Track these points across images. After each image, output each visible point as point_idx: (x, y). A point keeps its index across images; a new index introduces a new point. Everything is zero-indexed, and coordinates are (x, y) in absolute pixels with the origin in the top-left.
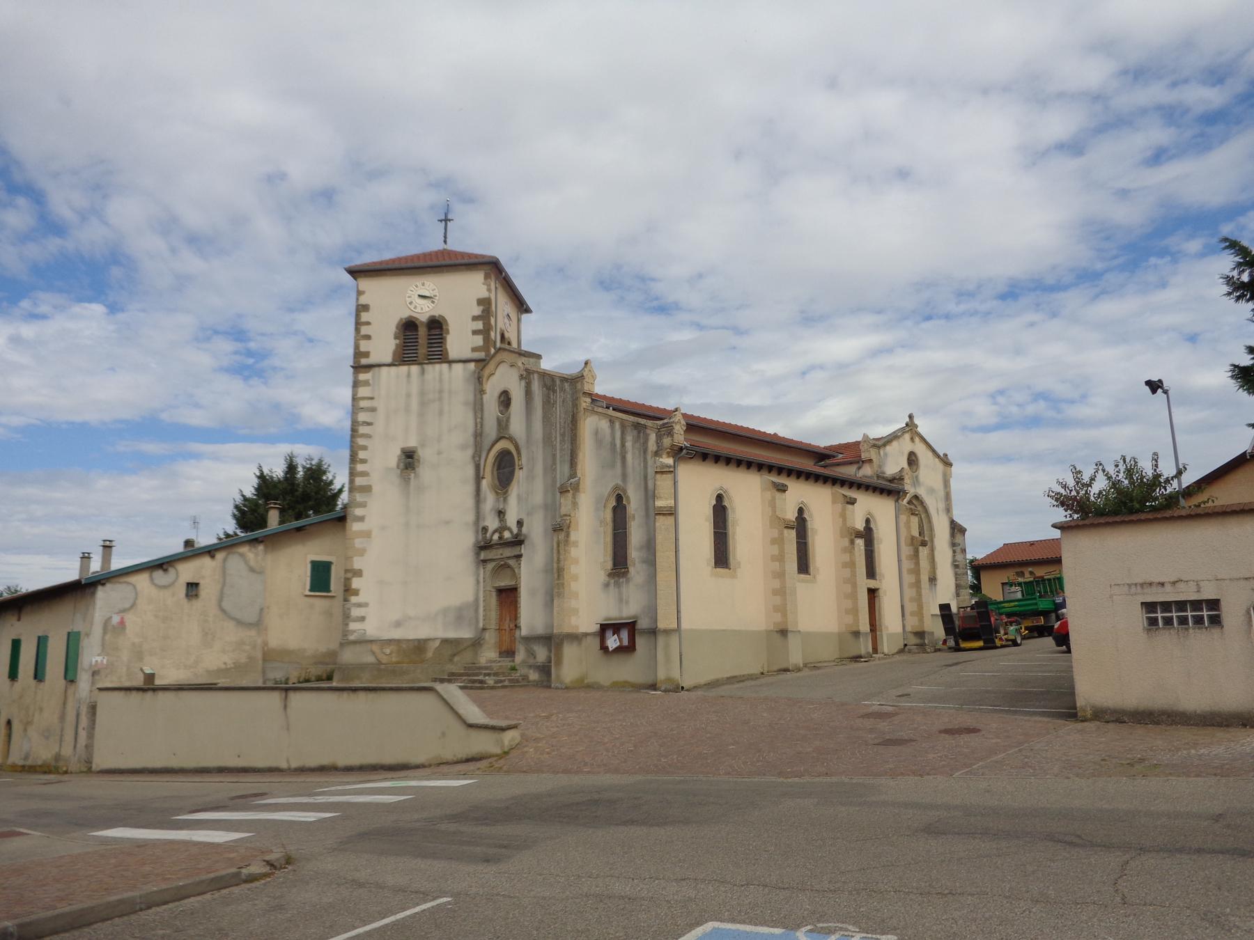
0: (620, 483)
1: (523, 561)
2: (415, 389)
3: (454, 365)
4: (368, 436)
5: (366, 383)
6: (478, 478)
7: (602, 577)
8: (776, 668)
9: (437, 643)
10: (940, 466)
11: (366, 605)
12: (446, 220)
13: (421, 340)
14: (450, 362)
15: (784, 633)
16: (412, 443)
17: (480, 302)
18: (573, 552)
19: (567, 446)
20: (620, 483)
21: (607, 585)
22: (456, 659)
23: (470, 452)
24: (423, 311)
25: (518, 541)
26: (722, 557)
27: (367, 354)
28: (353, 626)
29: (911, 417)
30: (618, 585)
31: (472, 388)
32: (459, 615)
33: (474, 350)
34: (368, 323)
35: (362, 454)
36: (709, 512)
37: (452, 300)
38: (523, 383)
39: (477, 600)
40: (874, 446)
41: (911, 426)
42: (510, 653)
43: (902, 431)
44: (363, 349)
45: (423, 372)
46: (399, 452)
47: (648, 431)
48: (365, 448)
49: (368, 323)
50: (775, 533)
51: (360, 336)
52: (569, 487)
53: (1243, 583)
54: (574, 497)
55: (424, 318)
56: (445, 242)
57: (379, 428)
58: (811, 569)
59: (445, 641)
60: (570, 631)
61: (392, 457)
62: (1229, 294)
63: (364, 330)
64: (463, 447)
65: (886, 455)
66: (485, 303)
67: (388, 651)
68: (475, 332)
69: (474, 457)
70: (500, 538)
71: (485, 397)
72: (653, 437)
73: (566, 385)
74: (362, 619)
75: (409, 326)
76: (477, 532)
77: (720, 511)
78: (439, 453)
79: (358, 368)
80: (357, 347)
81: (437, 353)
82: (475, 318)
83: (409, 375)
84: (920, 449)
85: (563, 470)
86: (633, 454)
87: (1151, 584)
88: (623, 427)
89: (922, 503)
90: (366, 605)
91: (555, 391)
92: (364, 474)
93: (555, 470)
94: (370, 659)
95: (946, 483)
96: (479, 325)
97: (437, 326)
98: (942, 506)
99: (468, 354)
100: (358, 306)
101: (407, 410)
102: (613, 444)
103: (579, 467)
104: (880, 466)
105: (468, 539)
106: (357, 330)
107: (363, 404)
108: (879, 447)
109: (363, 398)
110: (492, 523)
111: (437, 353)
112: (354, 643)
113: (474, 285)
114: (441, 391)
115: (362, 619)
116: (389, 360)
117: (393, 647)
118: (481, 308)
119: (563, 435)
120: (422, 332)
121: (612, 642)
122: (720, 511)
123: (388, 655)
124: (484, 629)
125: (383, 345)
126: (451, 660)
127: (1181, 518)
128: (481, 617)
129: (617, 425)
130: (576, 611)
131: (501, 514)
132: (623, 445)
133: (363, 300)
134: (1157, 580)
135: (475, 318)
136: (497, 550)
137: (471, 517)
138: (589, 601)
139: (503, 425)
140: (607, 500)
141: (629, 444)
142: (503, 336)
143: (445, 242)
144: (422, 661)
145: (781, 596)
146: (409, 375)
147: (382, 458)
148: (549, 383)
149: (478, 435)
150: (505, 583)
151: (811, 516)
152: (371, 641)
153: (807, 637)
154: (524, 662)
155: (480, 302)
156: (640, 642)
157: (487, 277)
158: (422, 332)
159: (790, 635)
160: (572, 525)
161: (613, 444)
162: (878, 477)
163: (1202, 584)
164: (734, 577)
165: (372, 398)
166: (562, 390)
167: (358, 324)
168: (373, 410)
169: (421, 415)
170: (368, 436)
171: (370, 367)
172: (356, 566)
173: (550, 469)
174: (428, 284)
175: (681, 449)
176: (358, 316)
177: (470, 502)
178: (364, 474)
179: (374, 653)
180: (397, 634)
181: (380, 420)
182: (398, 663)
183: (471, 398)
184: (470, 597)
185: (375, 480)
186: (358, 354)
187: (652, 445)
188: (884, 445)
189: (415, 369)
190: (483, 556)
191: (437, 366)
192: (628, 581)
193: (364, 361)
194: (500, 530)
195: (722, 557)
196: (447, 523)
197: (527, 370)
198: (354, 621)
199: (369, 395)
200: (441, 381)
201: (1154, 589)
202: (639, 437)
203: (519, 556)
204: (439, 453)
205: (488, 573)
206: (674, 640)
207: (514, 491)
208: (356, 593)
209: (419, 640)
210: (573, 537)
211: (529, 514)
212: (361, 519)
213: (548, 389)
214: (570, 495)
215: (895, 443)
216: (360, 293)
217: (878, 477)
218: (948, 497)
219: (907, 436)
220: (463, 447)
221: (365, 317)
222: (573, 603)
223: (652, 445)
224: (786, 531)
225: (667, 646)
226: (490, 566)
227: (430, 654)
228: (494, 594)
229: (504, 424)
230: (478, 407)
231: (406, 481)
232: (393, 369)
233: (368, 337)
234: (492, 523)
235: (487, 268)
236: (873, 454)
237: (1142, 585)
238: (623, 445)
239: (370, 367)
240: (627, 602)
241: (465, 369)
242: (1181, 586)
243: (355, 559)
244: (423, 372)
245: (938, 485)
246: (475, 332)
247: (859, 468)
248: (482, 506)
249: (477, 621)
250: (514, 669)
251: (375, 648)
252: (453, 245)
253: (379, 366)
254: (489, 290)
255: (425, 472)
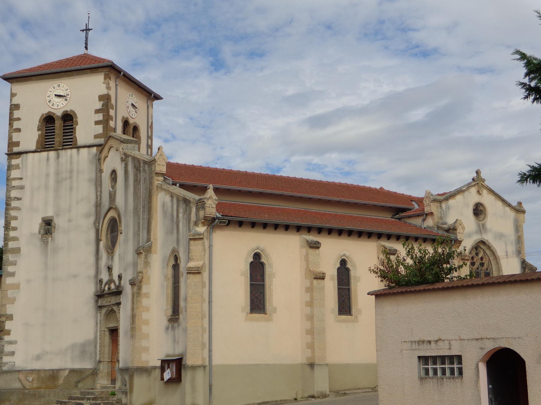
0: (176, 246)
1: (122, 306)
2: (52, 171)
3: (81, 150)
4: (18, 209)
5: (17, 167)
6: (98, 240)
7: (165, 322)
8: (307, 395)
9: (66, 373)
10: (512, 214)
11: (15, 342)
12: (87, 30)
13: (57, 130)
14: (78, 148)
15: (312, 365)
16: (50, 213)
17: (101, 98)
18: (145, 302)
19: (146, 216)
20: (176, 246)
21: (167, 328)
22: (80, 385)
23: (92, 219)
24: (58, 107)
25: (118, 293)
26: (258, 302)
27: (17, 144)
28: (5, 359)
29: (478, 172)
30: (173, 328)
31: (94, 168)
32: (83, 350)
33: (96, 137)
34: (19, 119)
35: (13, 224)
36: (246, 269)
37: (81, 96)
38: (123, 165)
39: (96, 338)
40: (435, 201)
41: (478, 181)
42: (113, 381)
43: (469, 186)
44: (14, 140)
45: (58, 156)
46: (40, 221)
47: (192, 205)
48: (16, 218)
49: (19, 119)
50: (307, 283)
51: (13, 130)
52: (143, 250)
53: (474, 342)
54: (146, 257)
55: (59, 113)
56: (86, 48)
57: (25, 203)
58: (353, 311)
59: (72, 371)
60: (140, 365)
61: (36, 225)
62: (526, 97)
63: (16, 125)
64: (88, 216)
65: (448, 208)
66: (105, 99)
67: (31, 379)
68: (97, 123)
69: (95, 223)
70: (109, 289)
71: (103, 174)
72: (194, 210)
73: (146, 166)
74: (13, 353)
75: (48, 120)
76: (97, 284)
77: (257, 267)
78: (69, 221)
79: (11, 155)
80: (10, 138)
81: (69, 142)
82: (97, 111)
83: (48, 159)
84: (487, 200)
85: (143, 234)
86: (183, 222)
87: (423, 342)
88: (178, 200)
89: (489, 247)
90: (15, 342)
91: (140, 172)
92: (15, 239)
93: (139, 235)
94: (17, 385)
95: (518, 228)
96: (100, 117)
97: (68, 118)
98: (512, 249)
99: (91, 141)
100: (11, 105)
101: (47, 187)
102: (172, 215)
103: (152, 233)
104: (441, 218)
105: (90, 289)
106: (11, 125)
107: (15, 183)
108: (440, 202)
109: (15, 179)
110: (105, 277)
111: (69, 142)
112: (6, 372)
113: (95, 85)
114: (71, 172)
115: (13, 353)
116: (33, 147)
117: (34, 376)
118: (102, 102)
119: (144, 207)
120: (58, 124)
121: (167, 375)
122: (257, 267)
123: (30, 382)
124: (100, 362)
125: (29, 137)
126: (76, 386)
127: (444, 289)
128: (98, 353)
129: (175, 201)
130: (146, 349)
131: (110, 269)
132: (178, 216)
133: (15, 101)
134: (427, 339)
135: (97, 111)
136: (107, 297)
137: (92, 272)
138: (153, 344)
139: (112, 197)
140: (169, 260)
141: (181, 215)
142: (126, 123)
143: (86, 48)
144: (56, 387)
145: (314, 333)
146: (48, 159)
147: (28, 226)
148: (137, 165)
149: (98, 205)
150: (112, 325)
151: (354, 266)
152: (19, 371)
153: (332, 368)
154: (120, 389)
155: (101, 98)
156: (187, 376)
157: (107, 77)
158: (58, 124)
159: (316, 368)
160: (144, 280)
161: (172, 215)
162: (438, 227)
163: (452, 342)
164: (270, 320)
165: (21, 179)
166: (144, 171)
167: (12, 120)
168: (22, 188)
169: (57, 190)
170: (18, 209)
171: (20, 154)
172: (9, 312)
173: (137, 234)
174: (63, 86)
175: (214, 219)
176: (11, 114)
177: (92, 260)
178: (15, 239)
179: (20, 381)
180: (37, 366)
181: (26, 195)
182: (38, 388)
183: (93, 176)
184: (91, 336)
185: (22, 244)
186: (12, 144)
187: (193, 218)
188: (447, 199)
189: (52, 154)
190: (101, 302)
191: (69, 151)
192: (178, 326)
193: (16, 149)
194: (111, 281)
195: (258, 302)
196: (75, 276)
197: (125, 154)
198: (6, 355)
199: (20, 176)
200: (71, 163)
201: (426, 346)
202: (186, 209)
203: (119, 304)
204: (69, 221)
205: (102, 316)
206: (200, 375)
207: (118, 250)
208: (8, 333)
209: (53, 370)
210: (144, 289)
211: (125, 270)
212: (13, 274)
213: (137, 170)
214: (143, 256)
215: (459, 197)
216: (13, 95)
217: (438, 227)
218: (519, 240)
219: (473, 190)
220: (88, 216)
221: (16, 114)
222: (144, 343)
223: (193, 218)
224: (315, 282)
225: (193, 380)
226: (104, 311)
227: (61, 381)
228: (107, 333)
229: (112, 196)
230: (98, 183)
231: (45, 243)
232: (37, 154)
233: (19, 130)
234: (105, 277)
235: (106, 70)
236: (433, 208)
237: (418, 342)
238: (178, 216)
239: (20, 154)
240: (178, 343)
241: (89, 153)
242: (440, 343)
243: (8, 306)
244: (58, 156)
245: (508, 229)
246: (97, 123)
247: (424, 220)
248: (100, 262)
249: (96, 356)
250: (113, 394)
251: (21, 376)
252: (93, 51)
253: (27, 152)
254: (108, 88)
255: (59, 236)
